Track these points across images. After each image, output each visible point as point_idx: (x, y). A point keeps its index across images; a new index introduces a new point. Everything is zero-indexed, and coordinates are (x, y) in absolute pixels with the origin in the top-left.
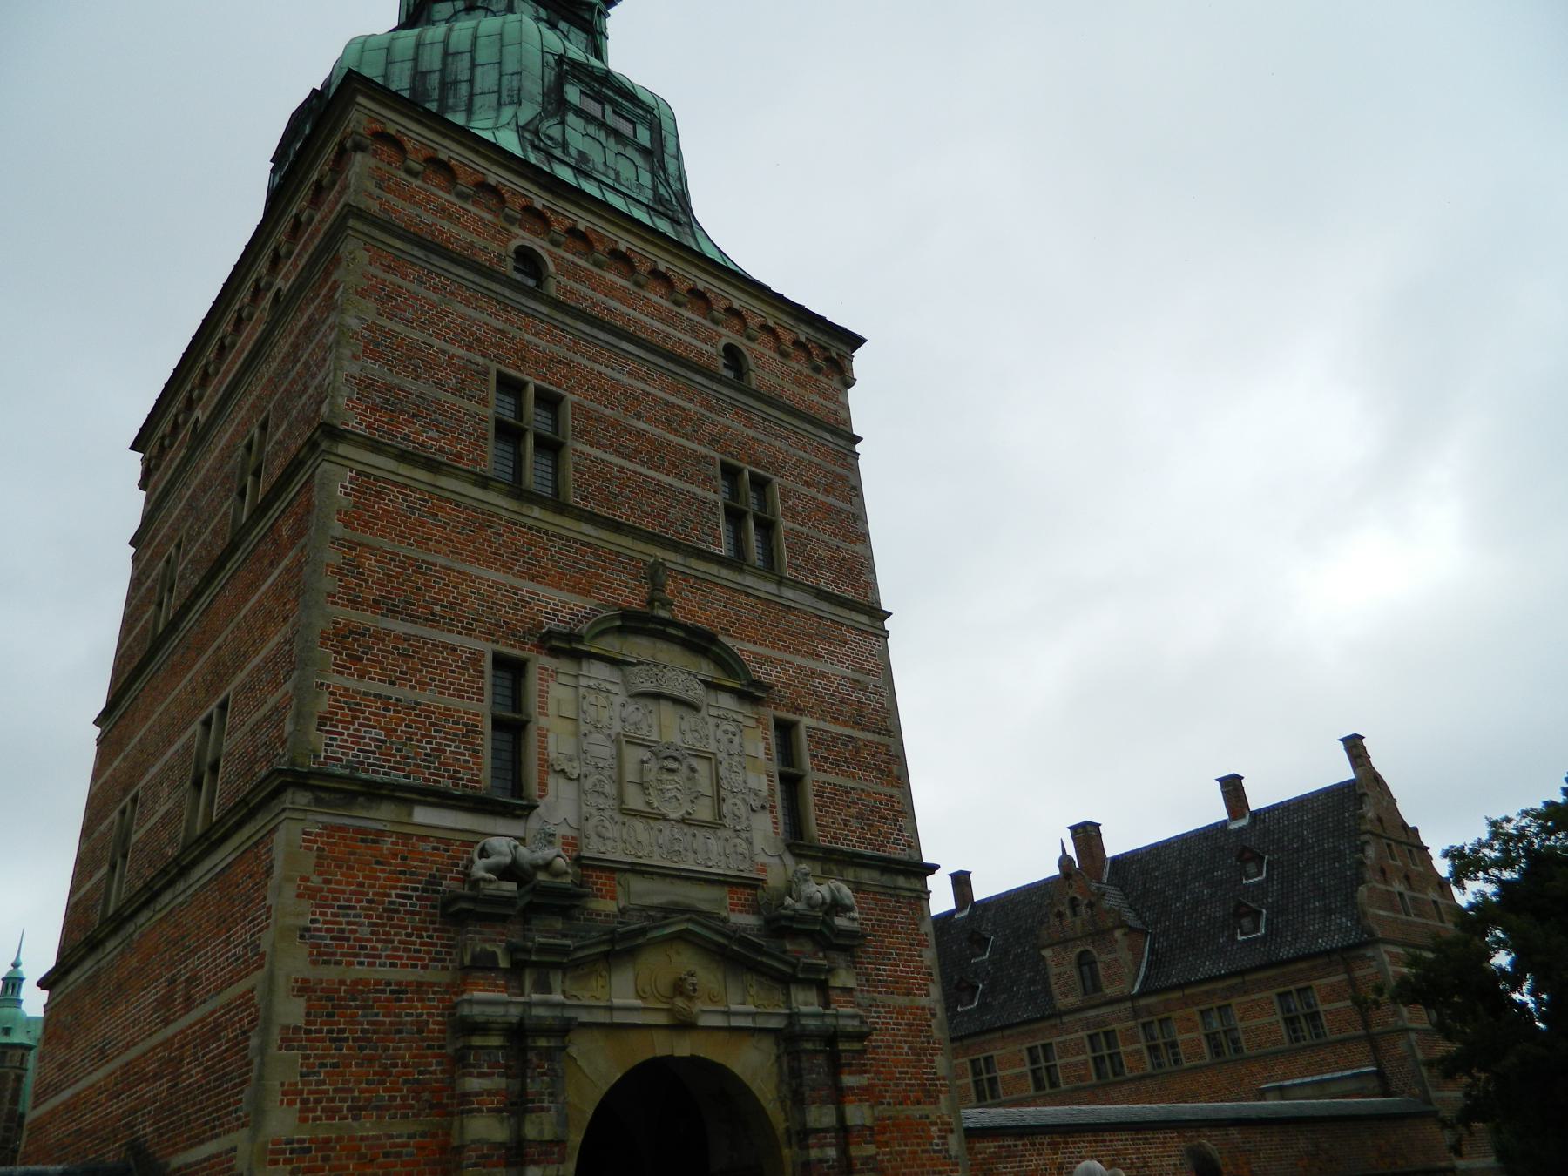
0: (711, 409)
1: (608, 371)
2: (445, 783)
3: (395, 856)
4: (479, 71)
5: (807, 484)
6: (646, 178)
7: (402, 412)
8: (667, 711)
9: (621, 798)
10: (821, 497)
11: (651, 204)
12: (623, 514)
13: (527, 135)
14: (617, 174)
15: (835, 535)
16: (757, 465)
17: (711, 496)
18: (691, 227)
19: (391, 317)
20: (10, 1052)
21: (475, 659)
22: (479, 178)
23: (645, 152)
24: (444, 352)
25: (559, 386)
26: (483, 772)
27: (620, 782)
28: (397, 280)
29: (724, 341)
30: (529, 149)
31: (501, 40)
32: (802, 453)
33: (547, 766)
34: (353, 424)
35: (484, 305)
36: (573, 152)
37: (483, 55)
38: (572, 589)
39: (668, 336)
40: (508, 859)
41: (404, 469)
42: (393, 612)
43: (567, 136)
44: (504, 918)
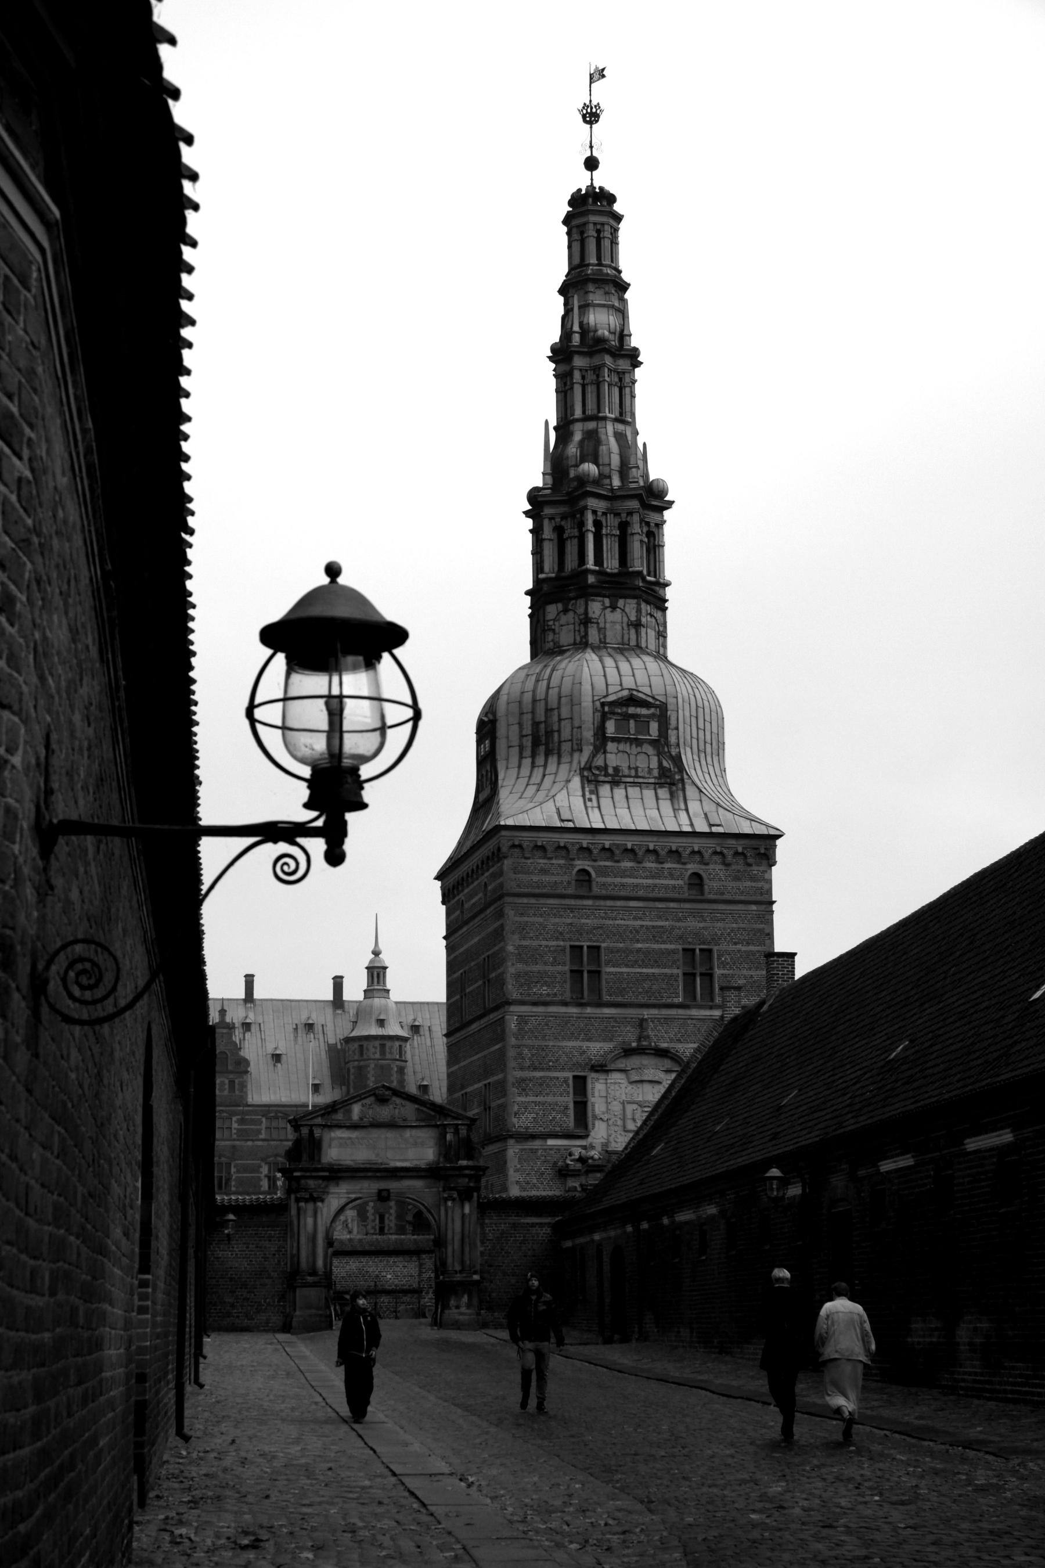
0: (679, 920)
1: (622, 922)
2: (558, 1129)
3: (542, 1156)
4: (563, 723)
5: (736, 944)
6: (654, 764)
7: (532, 982)
8: (647, 1087)
9: (624, 1126)
10: (744, 948)
11: (656, 781)
12: (629, 997)
13: (586, 774)
14: (636, 769)
15: (750, 969)
16: (704, 943)
17: (675, 971)
18: (682, 780)
19: (524, 938)
20: (388, 1044)
21: (566, 1080)
22: (556, 845)
23: (654, 743)
24: (546, 946)
25: (597, 941)
26: (569, 1121)
27: (624, 1119)
28: (526, 919)
29: (690, 872)
30: (586, 785)
31: (572, 700)
32: (734, 925)
33: (595, 1117)
34: (515, 995)
35: (562, 913)
36: (610, 771)
37: (565, 712)
38: (604, 1041)
39: (655, 886)
40: (577, 1157)
41: (535, 1009)
42: (535, 1069)
43: (608, 762)
44: (579, 1175)
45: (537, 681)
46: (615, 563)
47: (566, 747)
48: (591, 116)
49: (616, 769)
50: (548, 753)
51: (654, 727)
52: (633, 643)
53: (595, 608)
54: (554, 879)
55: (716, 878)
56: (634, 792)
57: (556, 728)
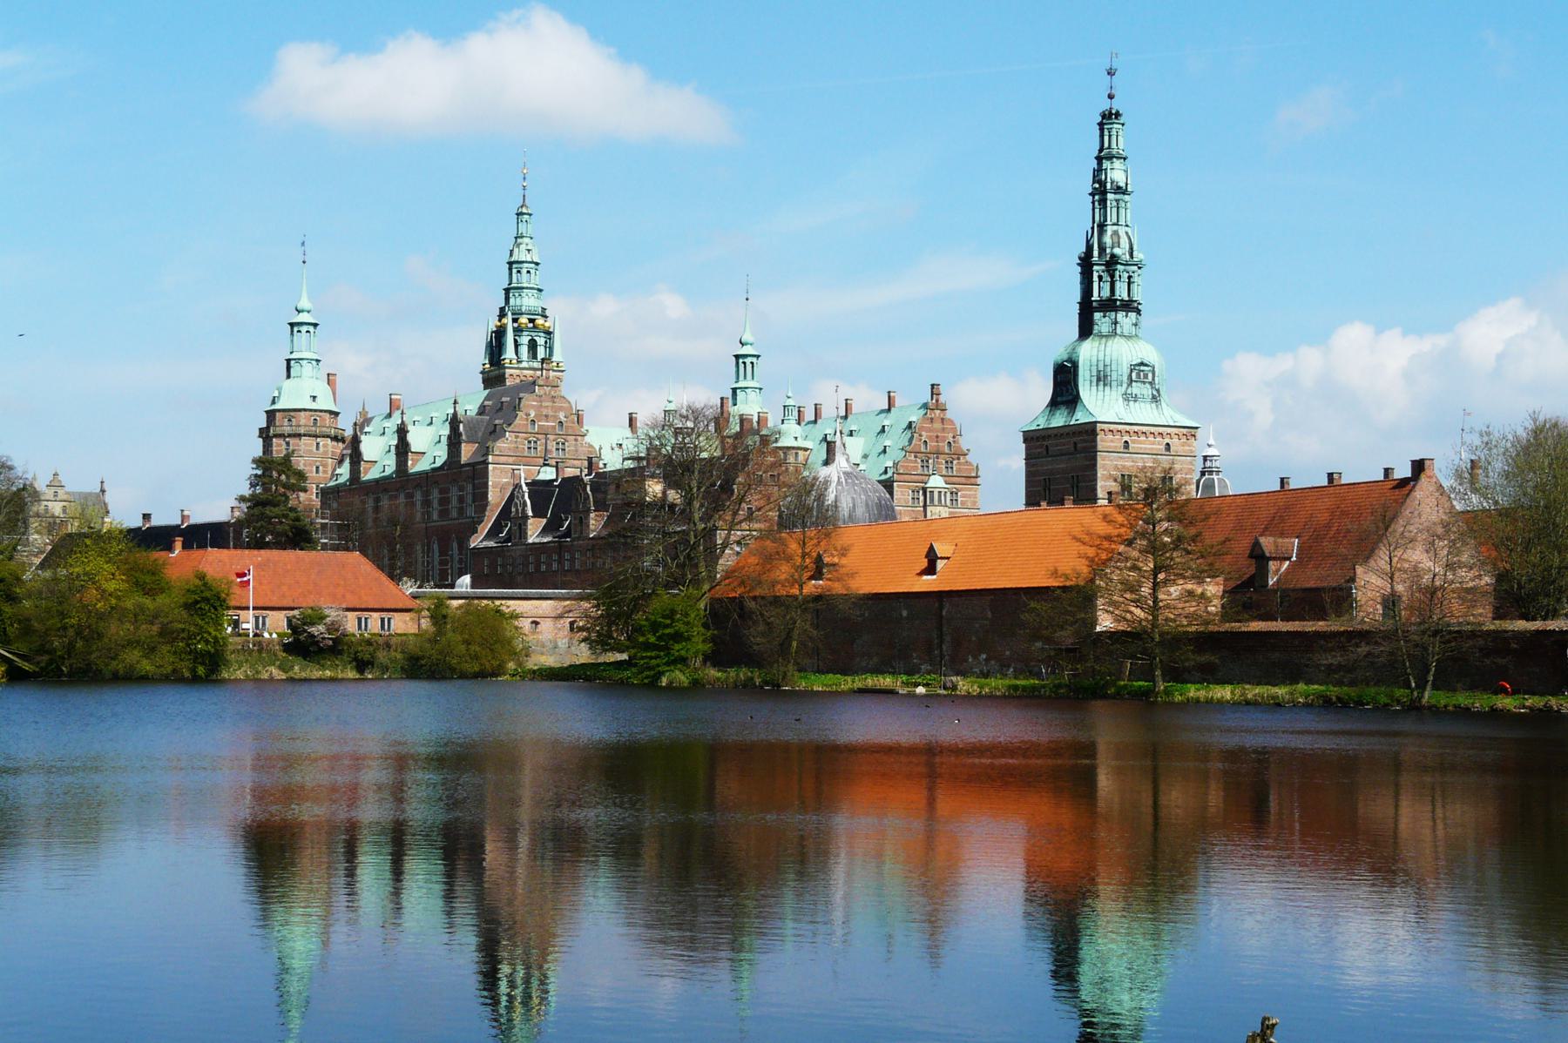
6: (1150, 393)
23: (1150, 383)
37: (1114, 367)
45: (1098, 351)
46: (1126, 294)
47: (1114, 384)
48: (1111, 73)
49: (1136, 395)
50: (1105, 385)
51: (1150, 375)
52: (1134, 333)
53: (1121, 315)
54: (1115, 444)
55: (1174, 442)
56: (1142, 404)
57: (1109, 374)
